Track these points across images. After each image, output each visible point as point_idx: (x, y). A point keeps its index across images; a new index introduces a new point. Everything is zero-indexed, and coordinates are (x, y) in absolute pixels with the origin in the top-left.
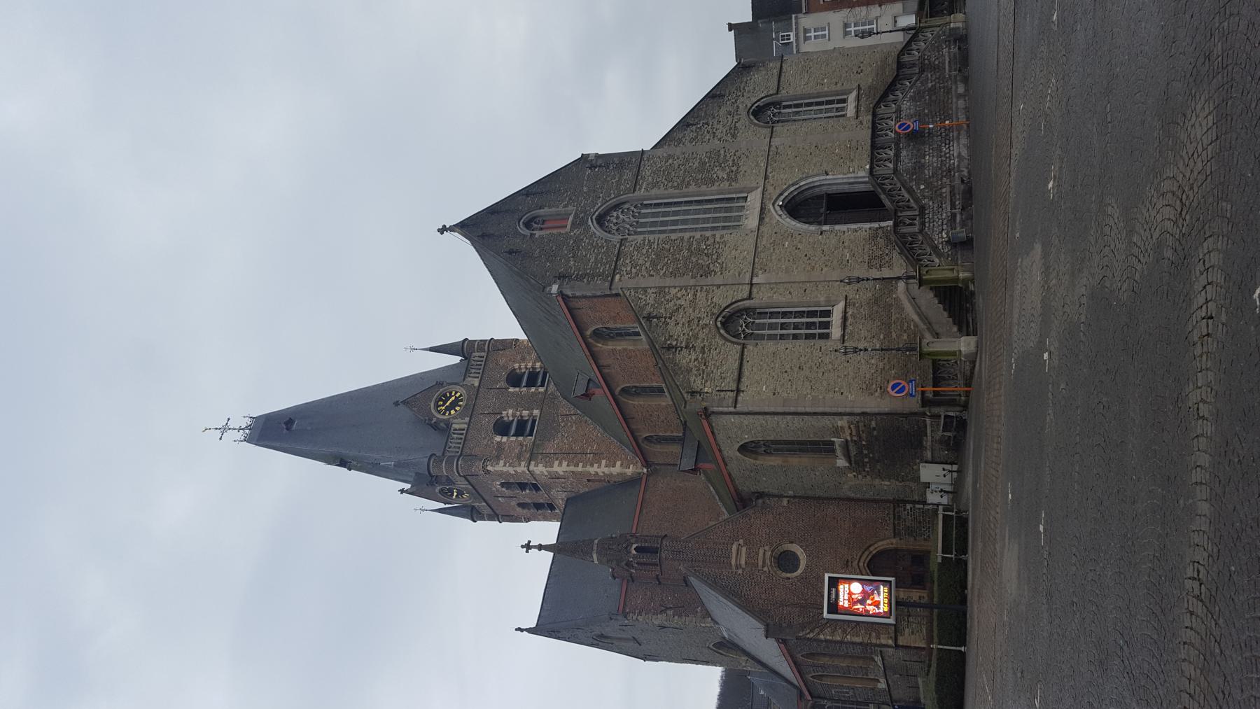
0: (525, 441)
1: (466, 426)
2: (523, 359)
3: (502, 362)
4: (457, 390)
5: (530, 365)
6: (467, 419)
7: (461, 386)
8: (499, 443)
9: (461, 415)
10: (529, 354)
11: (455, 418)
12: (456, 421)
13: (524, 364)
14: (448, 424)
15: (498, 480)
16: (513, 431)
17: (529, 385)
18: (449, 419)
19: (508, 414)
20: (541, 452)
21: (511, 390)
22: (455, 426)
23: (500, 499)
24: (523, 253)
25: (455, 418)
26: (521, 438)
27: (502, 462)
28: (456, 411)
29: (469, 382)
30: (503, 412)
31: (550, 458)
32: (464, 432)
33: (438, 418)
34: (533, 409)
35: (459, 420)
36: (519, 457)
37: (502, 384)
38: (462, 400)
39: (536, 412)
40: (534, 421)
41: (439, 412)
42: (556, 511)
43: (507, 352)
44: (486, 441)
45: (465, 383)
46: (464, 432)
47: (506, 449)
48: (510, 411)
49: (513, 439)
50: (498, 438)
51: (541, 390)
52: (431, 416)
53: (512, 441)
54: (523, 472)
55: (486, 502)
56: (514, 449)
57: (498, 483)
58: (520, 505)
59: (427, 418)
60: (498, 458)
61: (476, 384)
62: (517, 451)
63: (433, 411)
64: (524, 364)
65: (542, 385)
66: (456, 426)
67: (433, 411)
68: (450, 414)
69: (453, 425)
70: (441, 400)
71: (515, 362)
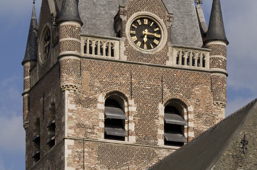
0: (98, 130)
1: (116, 58)
2: (199, 116)
3: (197, 90)
4: (162, 40)
5: (191, 124)
6: (124, 58)
7: (166, 45)
8: (95, 101)
9: (129, 51)
10: (206, 122)
11: (126, 42)
12: (123, 44)
13: (193, 118)
14: (119, 34)
15: (57, 100)
16: (110, 115)
17: (169, 128)
18: (125, 36)
19: (131, 106)
20: (86, 150)
21: (161, 107)
22: (117, 43)
23: (42, 99)
24: (242, 155)
25: (126, 42)
26: (102, 125)
27: (73, 107)
28: (136, 42)
29: (172, 54)
30: (133, 100)
31: (78, 162)
32: (110, 57)
33: (126, 22)
34: (137, 134)
35: (123, 48)
36: (80, 126)
37: (168, 95)
38: (149, 48)
39: (132, 139)
40: (122, 138)
41: (135, 22)
42: (34, 163)
43: (209, 95)
44: (99, 85)
45: (170, 48)
46: (110, 57)
47: (88, 109)
48: (133, 109)
49: (102, 117)
50: (102, 99)
51: (161, 142)
52: (128, 13)
53: (97, 115)
54: (63, 133)
55: (40, 80)
56: (89, 118)
57: (54, 101)
58: (38, 119)
59: (126, 9)
60: (78, 101)
61: (169, 63)
62: (87, 123)
63: (134, 15)
64: (193, 118)
65: (167, 143)
66: (116, 48)
67: (134, 15)
68: (132, 35)
69: (118, 42)
70: (150, 21)
71: (196, 106)
